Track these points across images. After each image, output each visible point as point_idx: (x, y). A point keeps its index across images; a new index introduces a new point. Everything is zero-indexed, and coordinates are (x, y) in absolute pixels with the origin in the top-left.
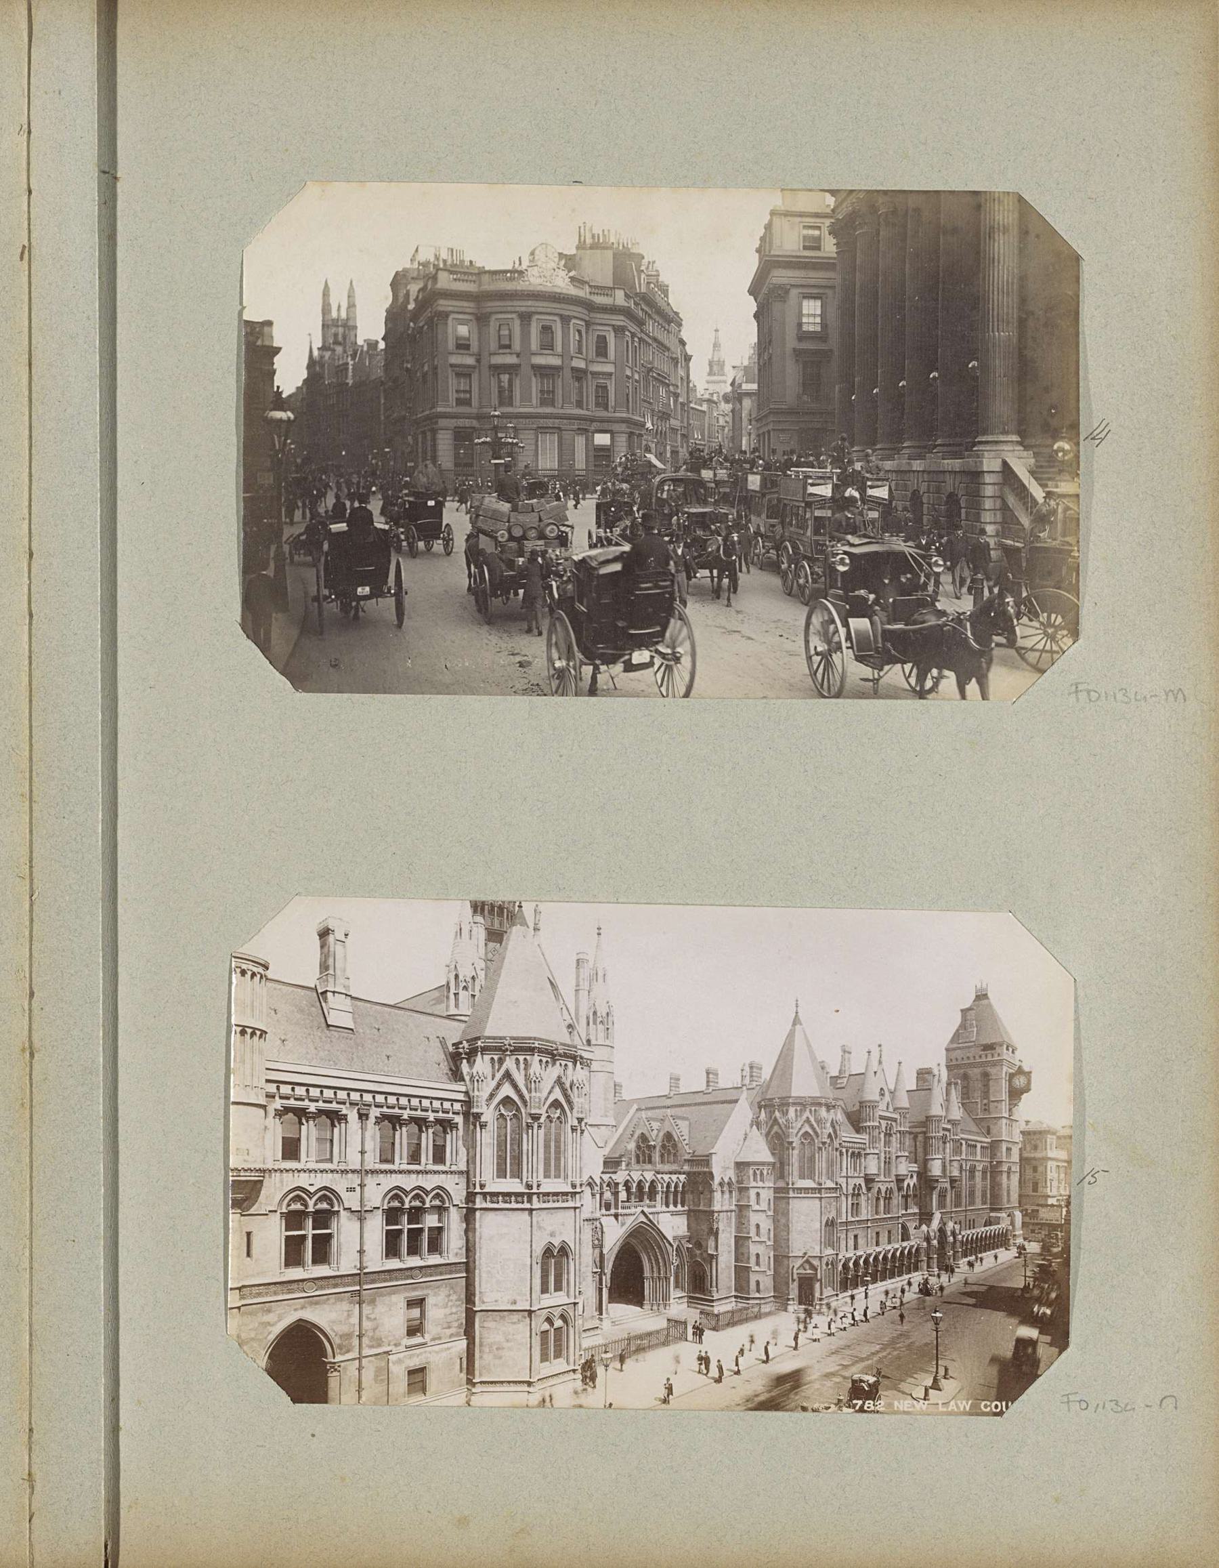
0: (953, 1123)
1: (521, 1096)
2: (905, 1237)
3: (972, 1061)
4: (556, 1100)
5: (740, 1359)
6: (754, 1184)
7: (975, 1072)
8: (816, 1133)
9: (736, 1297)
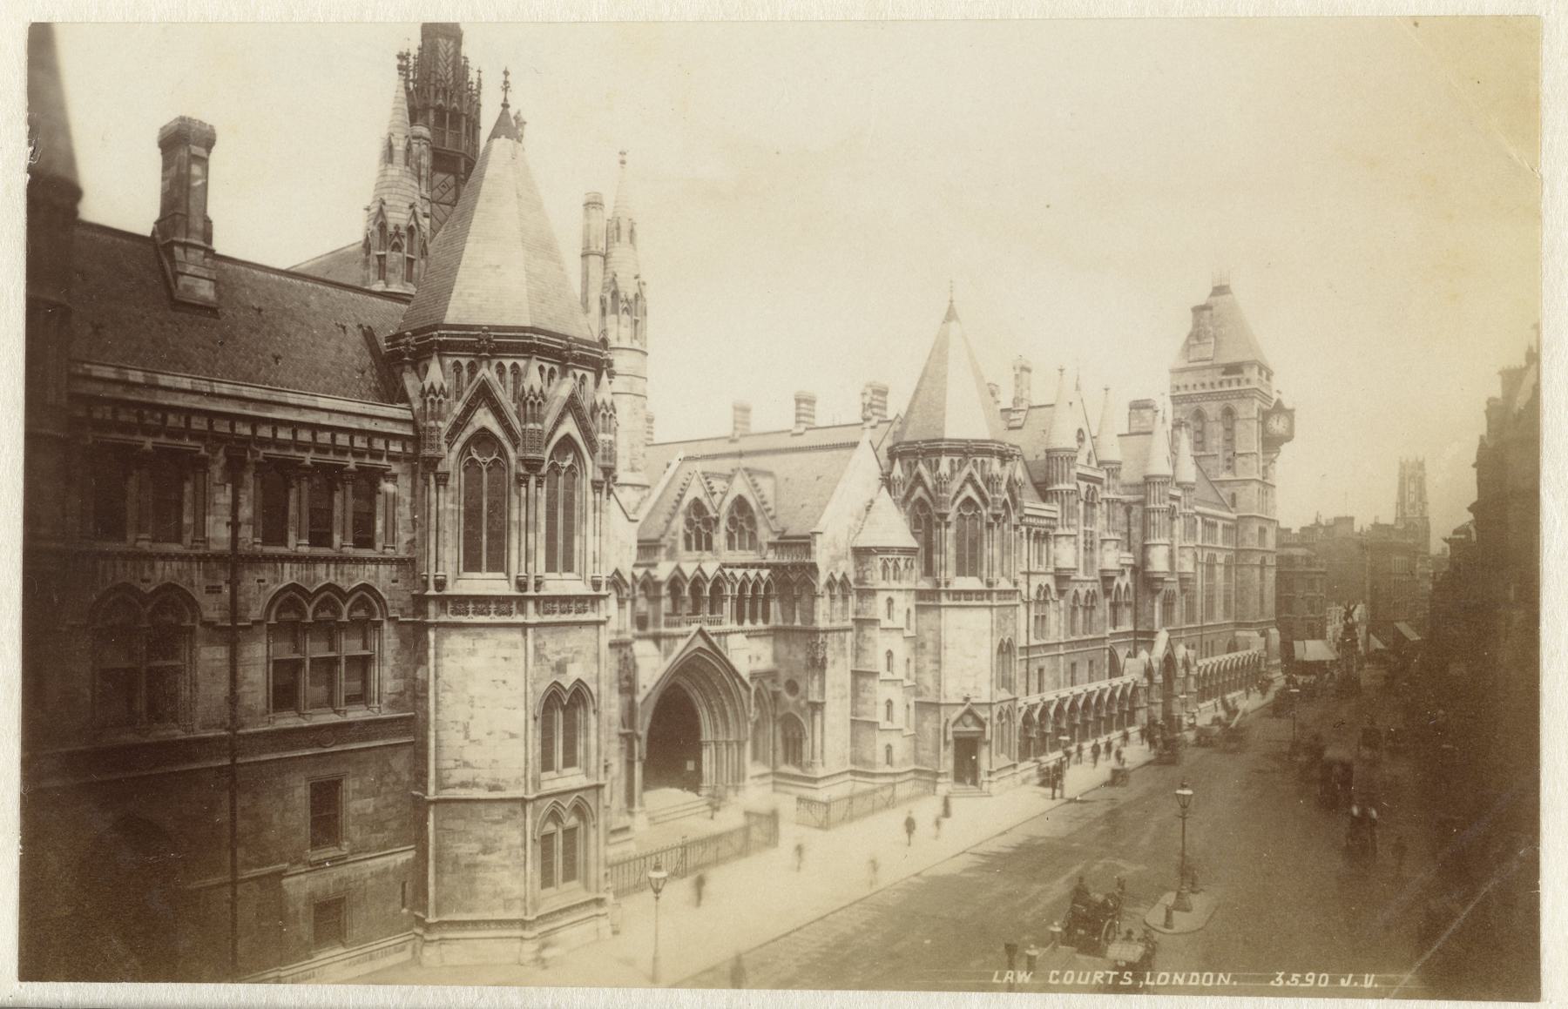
0: (1187, 488)
2: (1115, 670)
6: (884, 585)
7: (1213, 409)
8: (984, 500)
9: (853, 772)
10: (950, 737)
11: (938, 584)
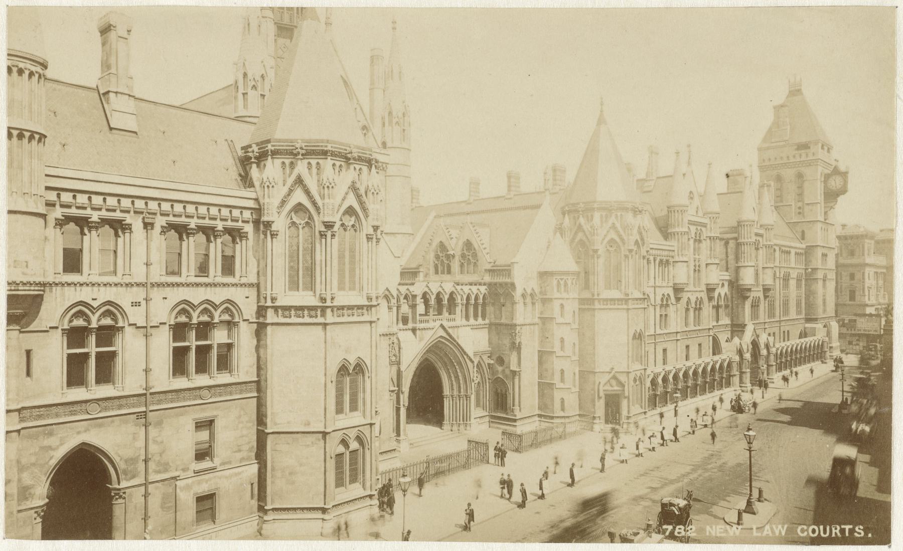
0: (768, 228)
1: (314, 203)
2: (716, 349)
3: (785, 160)
4: (351, 207)
5: (545, 483)
6: (557, 295)
7: (789, 174)
8: (622, 240)
9: (540, 416)
10: (602, 394)
11: (593, 295)
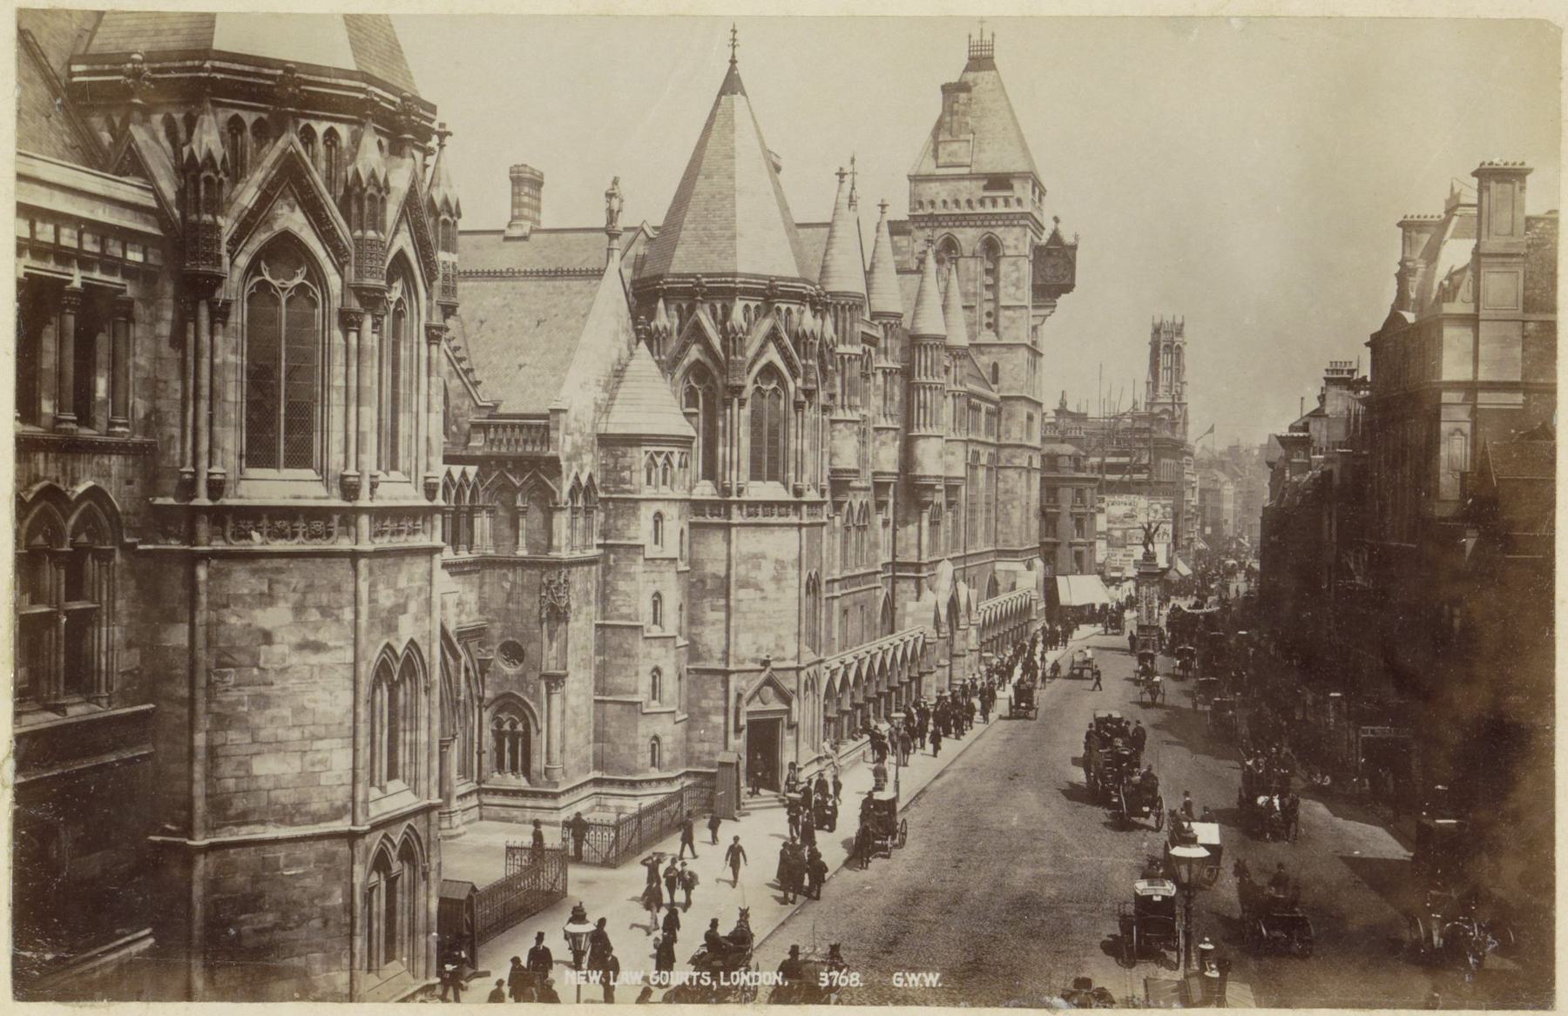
6: (648, 492)
7: (968, 237)
10: (743, 721)
11: (798, 492)
